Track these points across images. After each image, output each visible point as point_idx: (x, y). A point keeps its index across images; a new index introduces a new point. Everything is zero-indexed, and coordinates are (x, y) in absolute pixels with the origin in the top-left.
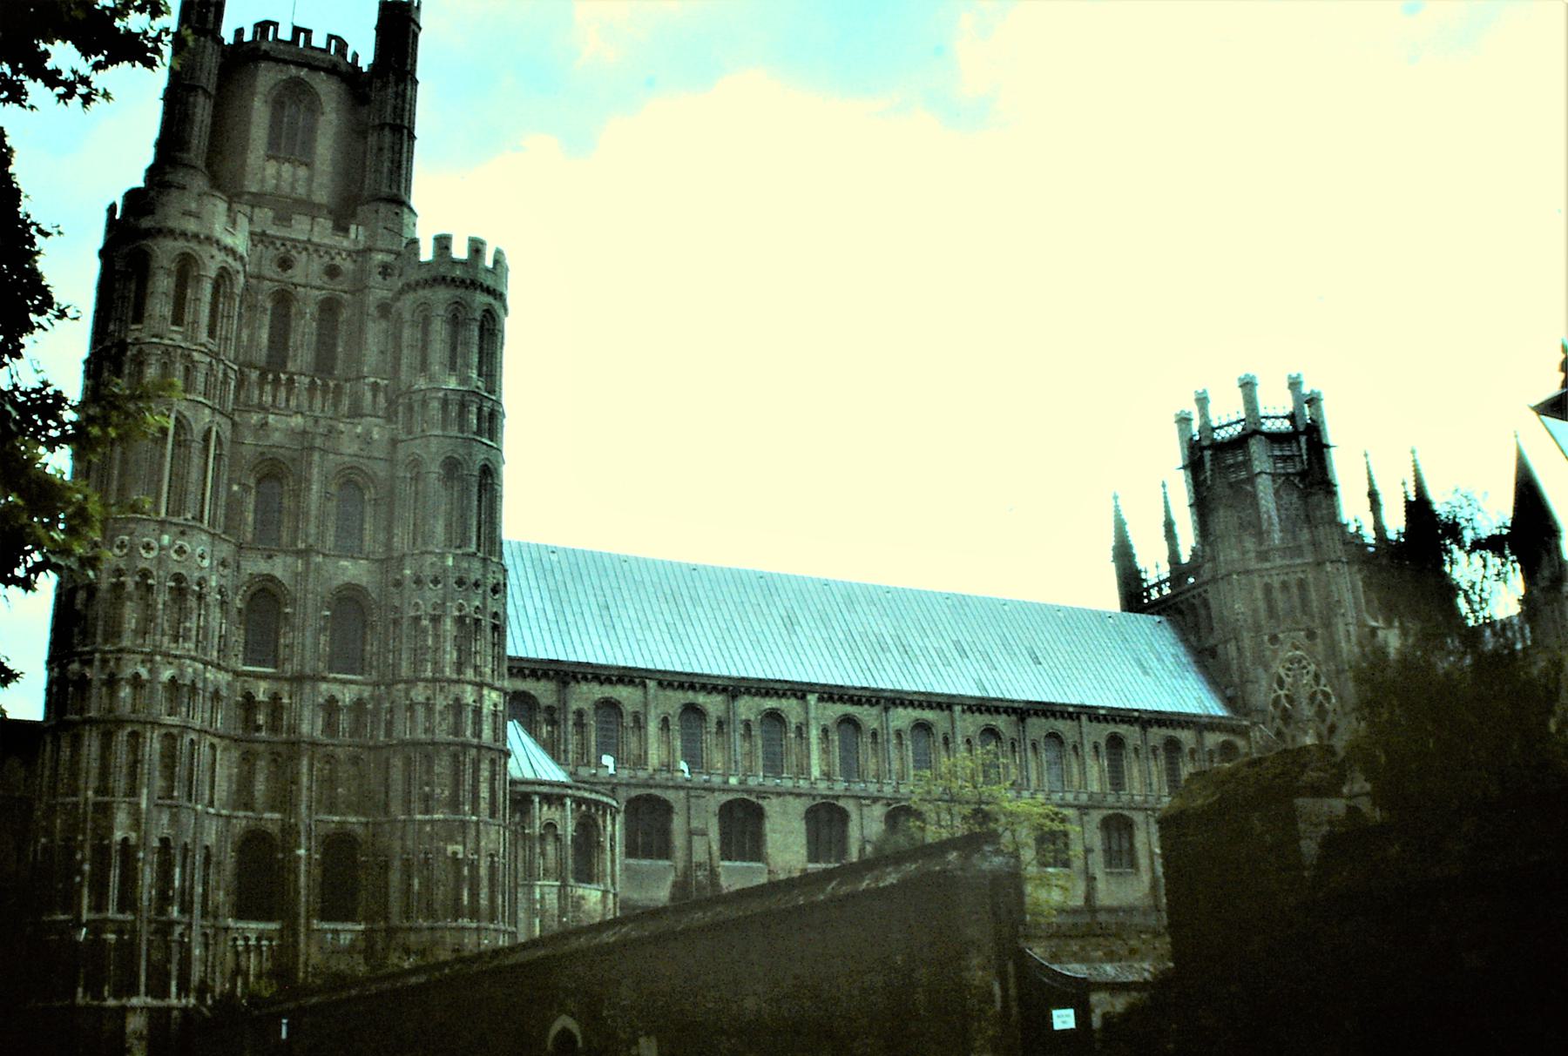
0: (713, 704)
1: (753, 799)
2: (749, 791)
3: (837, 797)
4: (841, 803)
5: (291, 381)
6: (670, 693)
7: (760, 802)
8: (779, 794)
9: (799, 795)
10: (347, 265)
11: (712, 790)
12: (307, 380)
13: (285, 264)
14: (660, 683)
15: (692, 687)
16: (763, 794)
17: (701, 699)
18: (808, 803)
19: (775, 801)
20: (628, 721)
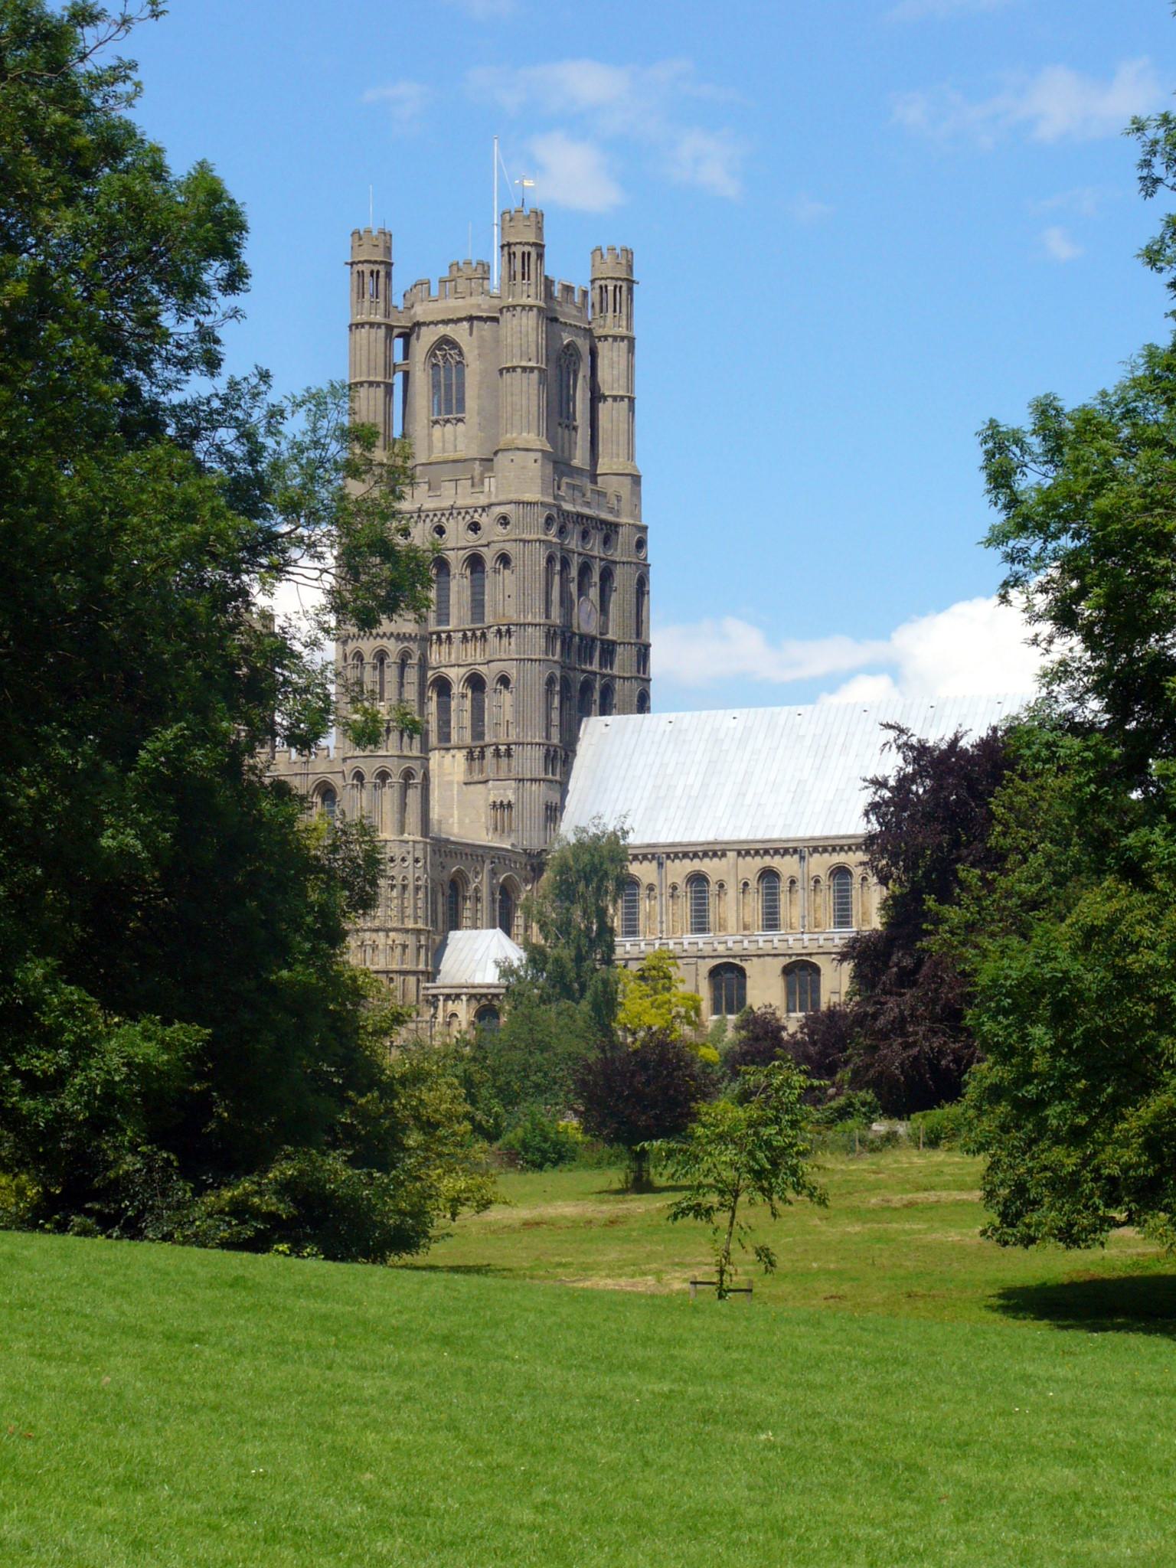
0: (787, 866)
1: (737, 961)
2: (734, 957)
3: (810, 954)
4: (814, 959)
5: (449, 637)
6: (749, 859)
7: (743, 964)
8: (759, 956)
9: (775, 955)
10: (484, 520)
11: (704, 957)
12: (460, 635)
13: (440, 530)
14: (739, 853)
15: (766, 852)
16: (744, 957)
17: (776, 862)
18: (787, 960)
19: (755, 959)
20: (713, 888)
